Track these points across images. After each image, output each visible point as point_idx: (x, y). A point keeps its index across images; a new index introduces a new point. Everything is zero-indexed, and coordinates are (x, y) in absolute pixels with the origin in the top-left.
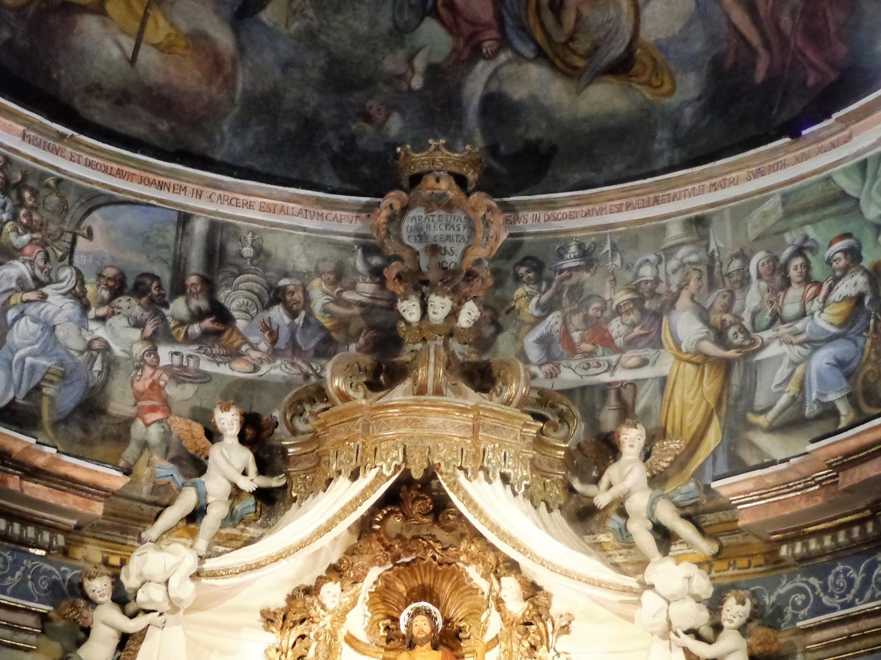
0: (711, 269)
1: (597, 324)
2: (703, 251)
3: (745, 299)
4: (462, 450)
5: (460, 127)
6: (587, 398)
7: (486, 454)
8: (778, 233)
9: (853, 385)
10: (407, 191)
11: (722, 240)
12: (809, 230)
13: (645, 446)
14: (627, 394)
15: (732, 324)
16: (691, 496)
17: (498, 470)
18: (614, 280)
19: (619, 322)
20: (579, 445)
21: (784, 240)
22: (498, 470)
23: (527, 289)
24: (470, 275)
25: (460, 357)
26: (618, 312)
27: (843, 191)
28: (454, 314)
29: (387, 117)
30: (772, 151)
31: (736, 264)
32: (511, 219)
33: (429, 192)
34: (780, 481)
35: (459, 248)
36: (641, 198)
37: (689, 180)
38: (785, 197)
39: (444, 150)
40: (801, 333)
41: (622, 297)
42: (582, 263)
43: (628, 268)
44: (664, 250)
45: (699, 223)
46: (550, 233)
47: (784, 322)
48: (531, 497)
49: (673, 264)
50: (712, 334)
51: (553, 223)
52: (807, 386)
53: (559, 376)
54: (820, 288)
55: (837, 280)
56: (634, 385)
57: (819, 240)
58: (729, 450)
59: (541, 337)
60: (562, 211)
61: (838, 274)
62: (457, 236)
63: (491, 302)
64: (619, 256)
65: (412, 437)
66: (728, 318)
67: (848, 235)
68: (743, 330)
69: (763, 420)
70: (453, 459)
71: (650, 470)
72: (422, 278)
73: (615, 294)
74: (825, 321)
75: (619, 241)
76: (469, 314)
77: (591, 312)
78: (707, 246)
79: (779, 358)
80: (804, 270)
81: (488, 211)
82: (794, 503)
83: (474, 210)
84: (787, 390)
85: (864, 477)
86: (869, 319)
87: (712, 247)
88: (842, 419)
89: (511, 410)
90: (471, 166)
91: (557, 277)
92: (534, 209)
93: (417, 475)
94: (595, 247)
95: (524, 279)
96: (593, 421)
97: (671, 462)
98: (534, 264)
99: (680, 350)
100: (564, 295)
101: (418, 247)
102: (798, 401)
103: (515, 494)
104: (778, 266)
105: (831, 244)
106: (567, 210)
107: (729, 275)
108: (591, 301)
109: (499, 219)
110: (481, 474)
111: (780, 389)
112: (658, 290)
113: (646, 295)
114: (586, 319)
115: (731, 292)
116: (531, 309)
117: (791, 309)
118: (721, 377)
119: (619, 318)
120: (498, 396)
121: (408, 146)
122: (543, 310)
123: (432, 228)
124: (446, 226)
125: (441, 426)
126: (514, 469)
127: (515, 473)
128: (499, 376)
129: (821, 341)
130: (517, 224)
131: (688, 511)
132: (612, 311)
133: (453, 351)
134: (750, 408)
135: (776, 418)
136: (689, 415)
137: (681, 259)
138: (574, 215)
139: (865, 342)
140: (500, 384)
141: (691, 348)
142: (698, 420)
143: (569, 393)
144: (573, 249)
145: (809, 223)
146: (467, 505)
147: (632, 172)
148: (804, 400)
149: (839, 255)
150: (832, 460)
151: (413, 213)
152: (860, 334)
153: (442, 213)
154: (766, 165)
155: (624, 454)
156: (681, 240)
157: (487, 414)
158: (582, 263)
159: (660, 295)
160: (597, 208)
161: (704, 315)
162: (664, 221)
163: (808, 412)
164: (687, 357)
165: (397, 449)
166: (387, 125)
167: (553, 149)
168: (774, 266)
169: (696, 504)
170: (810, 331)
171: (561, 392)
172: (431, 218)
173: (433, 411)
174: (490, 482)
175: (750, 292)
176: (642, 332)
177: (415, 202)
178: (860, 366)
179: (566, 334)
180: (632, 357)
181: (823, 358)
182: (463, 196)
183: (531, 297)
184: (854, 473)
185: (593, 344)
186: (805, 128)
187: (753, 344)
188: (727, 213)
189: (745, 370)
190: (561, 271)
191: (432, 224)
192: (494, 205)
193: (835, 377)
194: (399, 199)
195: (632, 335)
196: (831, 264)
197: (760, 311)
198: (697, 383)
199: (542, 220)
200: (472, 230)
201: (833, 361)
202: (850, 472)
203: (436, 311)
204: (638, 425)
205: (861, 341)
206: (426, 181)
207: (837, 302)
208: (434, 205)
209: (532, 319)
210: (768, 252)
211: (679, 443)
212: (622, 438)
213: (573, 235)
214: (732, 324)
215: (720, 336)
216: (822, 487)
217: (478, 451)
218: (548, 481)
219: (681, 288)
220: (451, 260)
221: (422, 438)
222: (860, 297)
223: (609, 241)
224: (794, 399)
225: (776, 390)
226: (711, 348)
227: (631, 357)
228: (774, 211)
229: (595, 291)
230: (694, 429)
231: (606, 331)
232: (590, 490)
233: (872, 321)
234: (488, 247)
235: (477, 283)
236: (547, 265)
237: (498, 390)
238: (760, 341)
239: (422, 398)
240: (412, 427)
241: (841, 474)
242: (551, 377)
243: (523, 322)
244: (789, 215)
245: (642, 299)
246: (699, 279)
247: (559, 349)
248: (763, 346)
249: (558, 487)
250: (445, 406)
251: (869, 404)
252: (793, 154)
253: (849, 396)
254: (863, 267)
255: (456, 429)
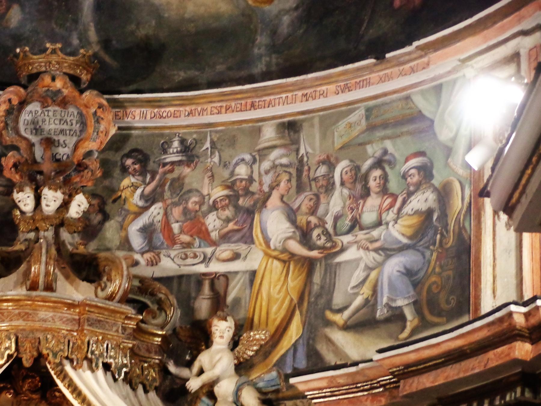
0: (299, 172)
1: (195, 217)
2: (294, 154)
3: (328, 203)
4: (69, 341)
5: (76, 21)
6: (184, 287)
7: (91, 347)
8: (361, 144)
9: (419, 293)
10: (25, 87)
11: (310, 146)
12: (388, 145)
13: (234, 335)
14: (220, 284)
15: (316, 226)
16: (273, 384)
17: (101, 361)
18: (213, 176)
19: (215, 217)
20: (174, 330)
21: (365, 151)
22: (101, 361)
23: (133, 180)
24: (81, 167)
25: (70, 248)
26: (214, 207)
27: (420, 111)
28: (65, 205)
29: (8, 9)
30: (358, 69)
31: (323, 170)
32: (120, 114)
33: (44, 89)
34: (350, 381)
35: (71, 141)
36: (239, 102)
37: (283, 89)
38: (369, 110)
39: (60, 53)
40: (376, 241)
41: (218, 193)
42: (184, 158)
43: (225, 166)
44: (259, 151)
45: (291, 128)
46: (156, 128)
47: (361, 229)
48: (129, 380)
49: (266, 165)
50: (298, 234)
51: (158, 120)
52: (379, 288)
53: (159, 264)
54: (395, 201)
55: (410, 194)
56: (226, 276)
57: (397, 155)
58: (308, 343)
59: (144, 226)
60: (167, 109)
61: (412, 188)
62: (70, 130)
63: (99, 191)
64: (217, 154)
65: (24, 330)
66: (313, 220)
67: (421, 154)
68: (326, 233)
69: (339, 319)
70: (61, 350)
71: (237, 358)
72: (36, 168)
73: (212, 189)
74: (398, 231)
75: (218, 139)
76: (79, 205)
77: (190, 205)
78: (298, 150)
79: (357, 261)
80: (382, 182)
81: (99, 107)
82: (361, 402)
83: (86, 106)
84: (361, 292)
85: (421, 387)
86: (435, 234)
87: (302, 151)
88: (408, 324)
89: (113, 305)
90: (84, 68)
91: (161, 170)
92: (142, 107)
93: (27, 362)
94: (196, 143)
95: (130, 170)
96: (187, 307)
97: (257, 352)
98: (140, 157)
99: (268, 246)
100: (166, 188)
101: (34, 139)
102: (370, 303)
103: (115, 380)
104: (359, 175)
105: (407, 160)
106: (172, 109)
107: (315, 179)
108: (191, 194)
109: (108, 115)
110: (85, 363)
111: (356, 291)
112: (252, 189)
113: (240, 192)
114: (186, 211)
115: (317, 196)
116: (136, 200)
117: (369, 217)
118: (304, 274)
119: (215, 213)
120: (103, 290)
121: (27, 49)
122: (146, 201)
123: (47, 122)
124: (60, 120)
125: (50, 319)
126: (115, 359)
127: (116, 363)
128: (104, 271)
129: (394, 250)
130: (126, 119)
131: (270, 396)
132: (209, 205)
133: (64, 241)
134: (329, 306)
135: (350, 318)
136: (274, 308)
137: (273, 162)
138: (178, 114)
139: (432, 255)
140: (105, 279)
141: (279, 246)
142: (282, 313)
143: (166, 281)
144: (176, 144)
145: (389, 138)
146: (72, 392)
147: (231, 74)
148: (375, 305)
149: (413, 171)
150: (395, 369)
151: (29, 108)
152: (428, 248)
153: (57, 108)
154: (353, 81)
155: (214, 343)
156: (274, 143)
157: (92, 310)
158: (184, 158)
159: (253, 194)
160: (199, 109)
161: (291, 215)
162: (260, 124)
163: (378, 314)
164: (275, 253)
165: (10, 339)
166: (7, 17)
167: (163, 47)
168: (356, 174)
169: (277, 391)
170: (385, 239)
171: (160, 280)
172: (46, 113)
173: (43, 306)
174: (93, 371)
175: (333, 197)
176: (236, 227)
177: (31, 97)
178: (427, 276)
179: (167, 225)
180: (226, 250)
181: (394, 265)
182: (76, 94)
183: (136, 188)
184: (413, 382)
185: (191, 236)
186: (389, 52)
187: (333, 247)
188: (316, 121)
189: (326, 270)
190: (165, 165)
191: (47, 119)
192: (105, 102)
193: (403, 284)
194: (17, 94)
195: (226, 230)
196: (406, 179)
197: (341, 216)
198: (283, 278)
199: (148, 117)
200: (83, 124)
201: (402, 270)
202: (410, 380)
203: (48, 203)
204: (229, 318)
205: (428, 253)
206: (43, 80)
207: (410, 215)
208: (50, 101)
209: (136, 209)
210: (351, 161)
211: (265, 334)
212: (214, 329)
213: (175, 131)
214: (316, 226)
215: (305, 236)
216: (386, 390)
217: (83, 342)
218: (146, 365)
219: (272, 188)
220: (63, 152)
221: (32, 331)
222: (429, 213)
223: (209, 139)
224: (367, 301)
225: (351, 292)
226: (295, 247)
227: (225, 250)
228: (358, 123)
229: (195, 185)
230: (277, 322)
231: (203, 224)
232: (184, 372)
233: (438, 236)
234: (98, 141)
235: (87, 174)
236: (152, 159)
237: (103, 285)
238: (340, 245)
239: (34, 293)
240: (24, 320)
241: (402, 381)
242: (152, 265)
243: (128, 212)
244: (371, 128)
245: (237, 197)
246: (289, 181)
247: (159, 238)
248: (343, 250)
249: (154, 371)
250: (55, 302)
251: (432, 313)
252: (377, 74)
253: (415, 303)
254: (433, 185)
255: (64, 323)
